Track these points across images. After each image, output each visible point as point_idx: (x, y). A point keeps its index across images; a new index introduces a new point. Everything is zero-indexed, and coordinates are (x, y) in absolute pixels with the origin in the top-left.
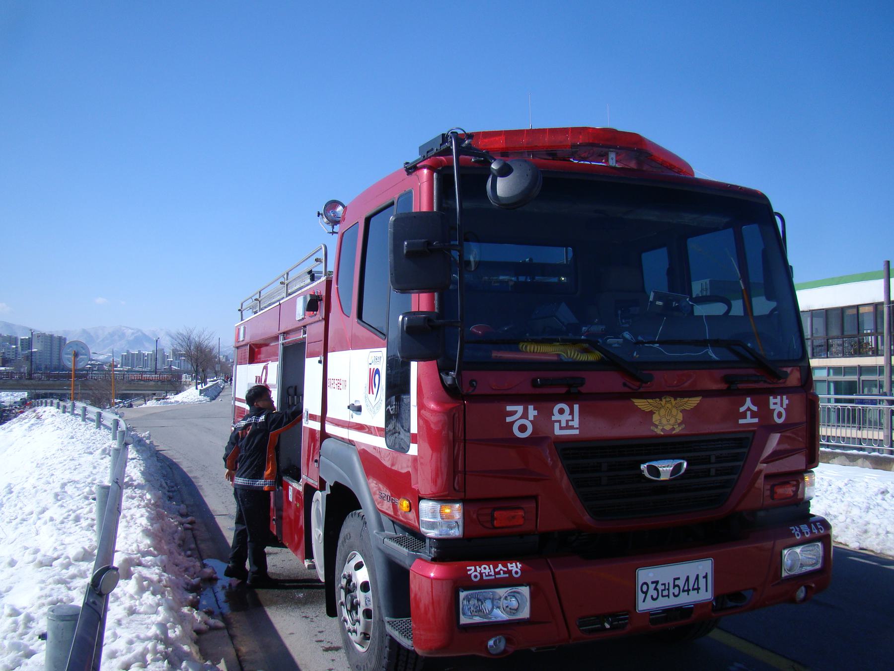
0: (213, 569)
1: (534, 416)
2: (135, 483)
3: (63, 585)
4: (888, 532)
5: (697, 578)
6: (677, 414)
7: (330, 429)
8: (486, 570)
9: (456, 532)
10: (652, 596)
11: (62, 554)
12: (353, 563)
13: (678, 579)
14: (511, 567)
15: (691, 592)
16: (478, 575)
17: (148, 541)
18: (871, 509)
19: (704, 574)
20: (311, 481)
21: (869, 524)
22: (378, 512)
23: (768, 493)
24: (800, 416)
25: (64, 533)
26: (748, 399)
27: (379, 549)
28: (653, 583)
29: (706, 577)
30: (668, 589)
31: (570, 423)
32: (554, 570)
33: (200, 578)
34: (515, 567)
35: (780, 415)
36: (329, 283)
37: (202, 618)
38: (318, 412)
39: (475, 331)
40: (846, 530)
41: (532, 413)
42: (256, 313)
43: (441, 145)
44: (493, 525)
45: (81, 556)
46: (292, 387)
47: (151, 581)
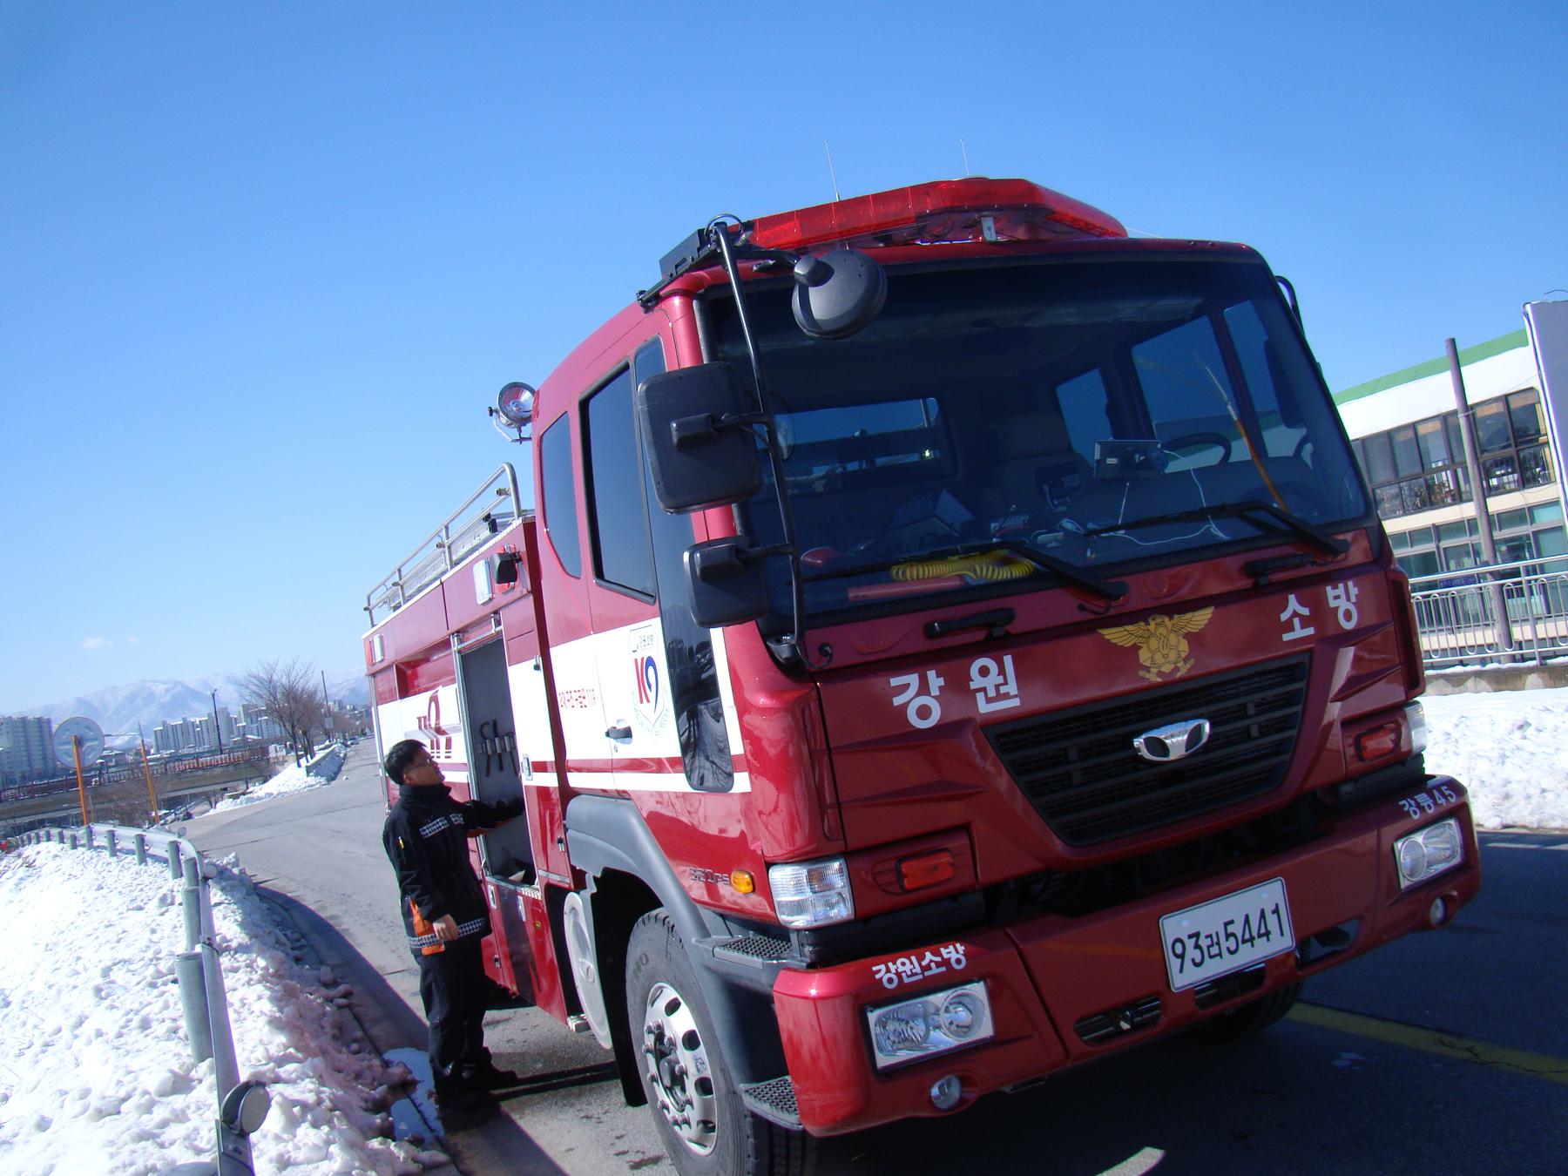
0: (405, 1066)
1: (939, 687)
2: (234, 944)
3: (150, 1142)
4: (1543, 791)
6: (1179, 643)
7: (575, 780)
8: (905, 967)
9: (842, 911)
10: (1193, 960)
11: (135, 1089)
12: (661, 1004)
13: (1232, 922)
14: (948, 953)
15: (1256, 942)
16: (894, 977)
17: (282, 1039)
18: (1508, 757)
19: (1274, 907)
20: (555, 879)
21: (1510, 782)
22: (692, 903)
23: (1351, 751)
25: (128, 1052)
26: (1292, 598)
27: (708, 969)
28: (1190, 937)
29: (1276, 911)
30: (1218, 944)
31: (1003, 690)
32: (1021, 946)
33: (385, 1086)
34: (954, 953)
35: (1348, 616)
36: (529, 529)
37: (406, 1152)
38: (549, 756)
39: (810, 560)
42: (395, 608)
43: (699, 250)
44: (903, 888)
45: (169, 1086)
46: (488, 723)
47: (305, 1107)
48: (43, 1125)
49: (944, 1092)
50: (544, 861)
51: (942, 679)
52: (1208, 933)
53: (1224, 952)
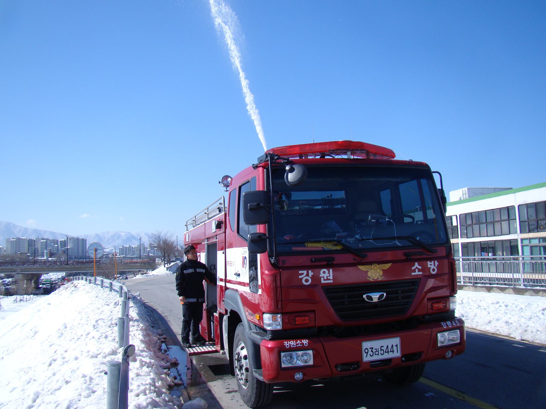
0: (176, 359)
1: (312, 275)
2: (134, 319)
3: (105, 365)
4: (538, 331)
7: (228, 285)
8: (292, 343)
9: (279, 328)
10: (370, 355)
11: (102, 352)
12: (240, 347)
13: (383, 346)
16: (289, 345)
17: (143, 345)
18: (532, 319)
19: (396, 345)
20: (221, 311)
21: (529, 326)
22: (248, 321)
23: (430, 307)
24: (446, 270)
25: (101, 343)
26: (416, 264)
27: (249, 338)
28: (370, 348)
30: (378, 351)
31: (329, 278)
32: (323, 343)
33: (169, 363)
34: (305, 342)
35: (434, 270)
36: (225, 215)
37: (171, 379)
38: (224, 278)
39: (286, 238)
40: (516, 330)
41: (311, 273)
42: (194, 227)
43: (266, 158)
44: (295, 324)
45: (111, 353)
46: (212, 265)
47: (146, 363)
48: (76, 359)
49: (299, 376)
50: (219, 306)
51: (313, 273)
52: (375, 348)
53: (380, 354)
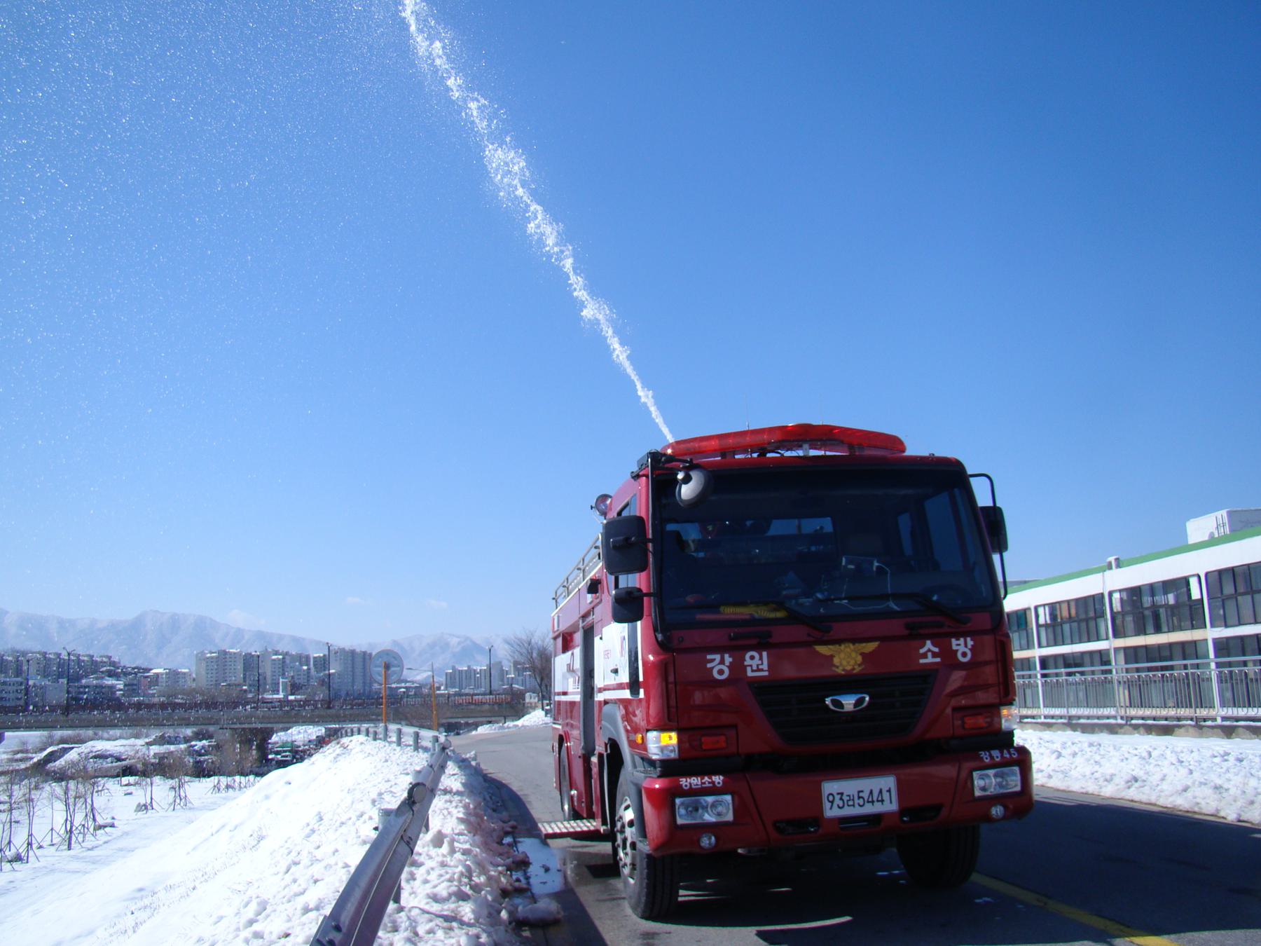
2: (454, 790)
5: (881, 791)
8: (695, 781)
12: (623, 806)
13: (862, 791)
15: (876, 803)
19: (888, 789)
24: (989, 654)
28: (838, 794)
29: (889, 791)
30: (853, 800)
31: (760, 667)
34: (718, 779)
35: (964, 654)
40: (1233, 803)
41: (728, 659)
49: (707, 841)
52: (848, 794)
53: (856, 805)
